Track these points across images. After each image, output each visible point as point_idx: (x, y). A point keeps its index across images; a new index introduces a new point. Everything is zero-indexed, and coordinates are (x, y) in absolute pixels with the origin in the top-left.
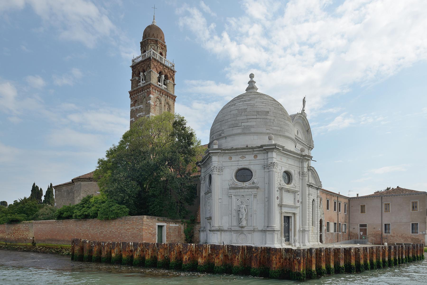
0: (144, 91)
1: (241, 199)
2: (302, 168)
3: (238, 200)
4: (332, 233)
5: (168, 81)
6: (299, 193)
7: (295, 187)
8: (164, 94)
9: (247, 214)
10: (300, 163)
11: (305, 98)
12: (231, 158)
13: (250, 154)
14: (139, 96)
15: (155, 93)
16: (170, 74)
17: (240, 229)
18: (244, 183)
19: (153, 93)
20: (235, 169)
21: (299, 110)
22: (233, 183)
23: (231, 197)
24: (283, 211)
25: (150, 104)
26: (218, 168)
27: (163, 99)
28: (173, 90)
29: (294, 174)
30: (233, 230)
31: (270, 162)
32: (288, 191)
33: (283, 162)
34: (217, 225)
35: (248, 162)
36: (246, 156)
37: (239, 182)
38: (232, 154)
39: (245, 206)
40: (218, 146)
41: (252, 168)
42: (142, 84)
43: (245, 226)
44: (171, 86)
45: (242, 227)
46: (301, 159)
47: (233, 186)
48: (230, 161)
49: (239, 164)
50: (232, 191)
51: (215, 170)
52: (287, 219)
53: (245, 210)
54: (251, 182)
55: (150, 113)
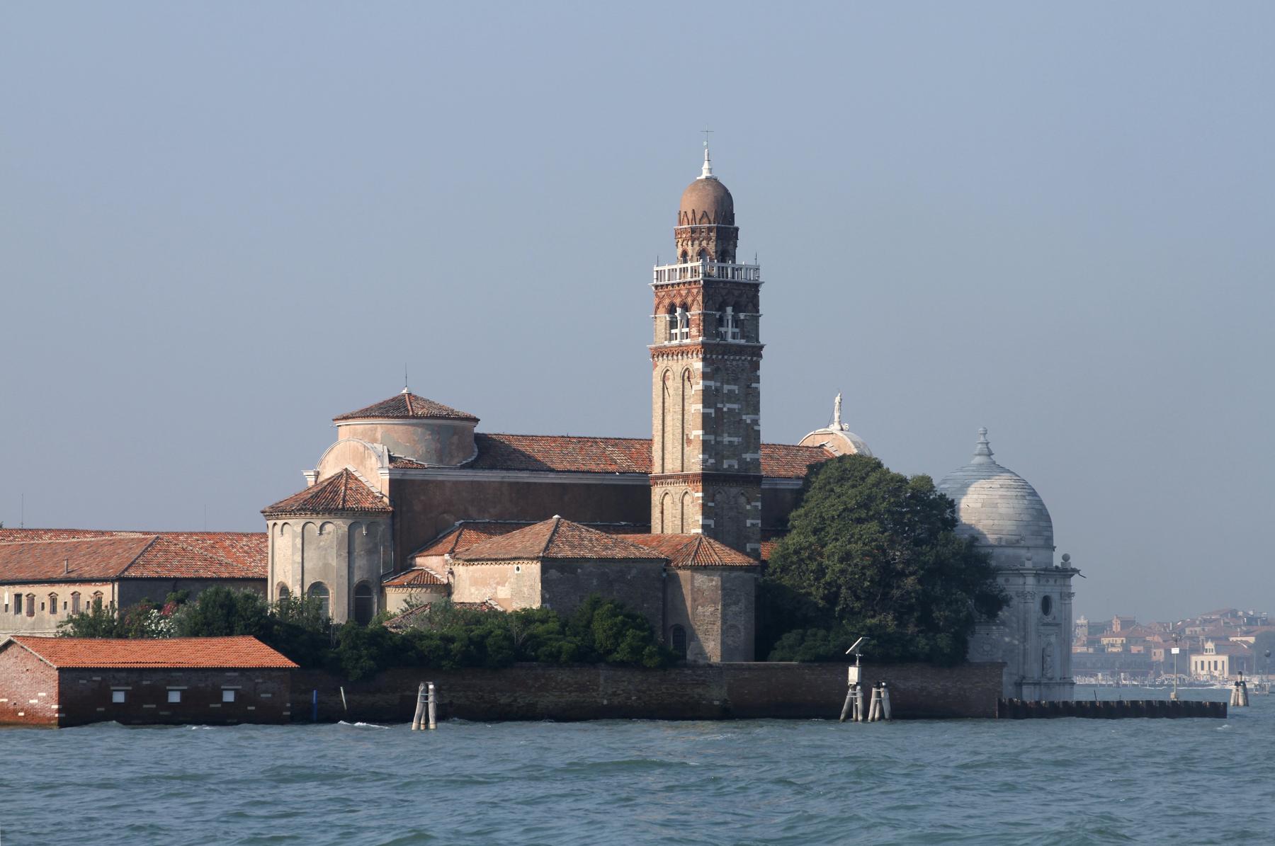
14: (728, 362)
20: (1042, 595)
45: (1051, 679)
50: (1042, 628)
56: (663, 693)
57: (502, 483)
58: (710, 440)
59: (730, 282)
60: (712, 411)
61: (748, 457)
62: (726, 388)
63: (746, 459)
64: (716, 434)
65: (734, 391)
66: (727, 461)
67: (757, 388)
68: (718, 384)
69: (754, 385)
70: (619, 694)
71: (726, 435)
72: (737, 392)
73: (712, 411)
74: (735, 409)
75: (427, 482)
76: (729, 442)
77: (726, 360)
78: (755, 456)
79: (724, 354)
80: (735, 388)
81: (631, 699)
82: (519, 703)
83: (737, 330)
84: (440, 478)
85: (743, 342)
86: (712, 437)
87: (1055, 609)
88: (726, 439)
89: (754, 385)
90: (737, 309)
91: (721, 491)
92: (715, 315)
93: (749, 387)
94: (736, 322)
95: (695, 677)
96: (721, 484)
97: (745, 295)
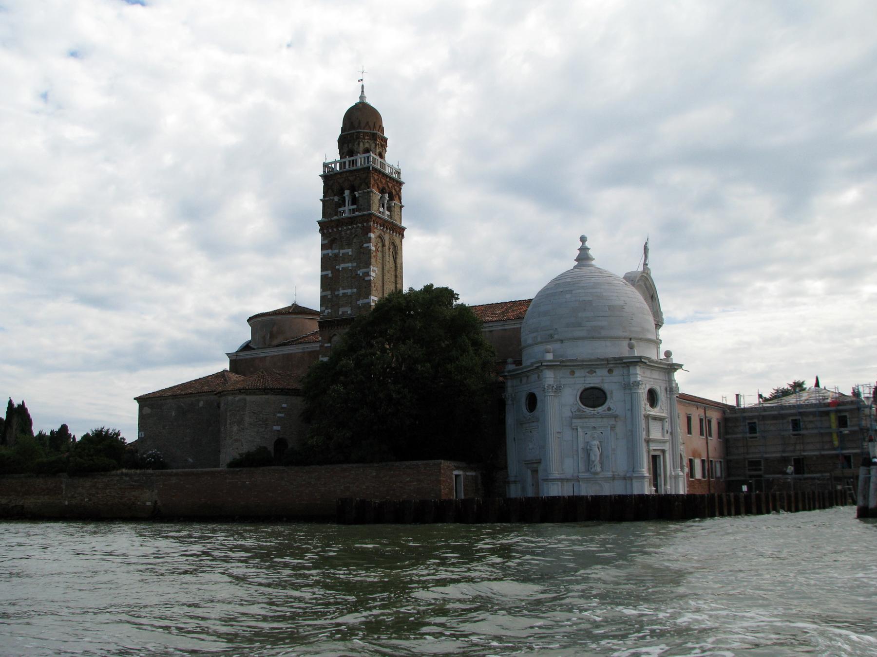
0: (356, 224)
2: (669, 381)
3: (586, 433)
4: (699, 480)
6: (667, 420)
7: (662, 411)
8: (388, 228)
9: (601, 455)
10: (666, 375)
11: (646, 243)
12: (573, 373)
13: (602, 368)
14: (343, 233)
15: (377, 228)
16: (395, 190)
17: (593, 476)
18: (596, 409)
20: (581, 388)
21: (636, 266)
22: (579, 410)
23: (577, 429)
24: (651, 448)
25: (369, 250)
26: (555, 387)
27: (387, 237)
28: (400, 216)
30: (581, 479)
31: (632, 380)
32: (655, 418)
33: (647, 377)
35: (601, 378)
36: (597, 370)
37: (587, 408)
39: (598, 442)
40: (553, 355)
41: (606, 387)
42: (347, 211)
44: (397, 209)
45: (596, 473)
46: (668, 368)
48: (571, 376)
51: (550, 390)
52: (655, 458)
53: (598, 448)
54: (605, 407)
55: (371, 266)
56: (108, 496)
57: (304, 353)
58: (327, 296)
59: (347, 172)
60: (329, 272)
61: (360, 302)
62: (342, 251)
63: (359, 305)
64: (333, 290)
65: (348, 253)
66: (342, 309)
67: (368, 247)
68: (337, 251)
69: (365, 245)
70: (76, 497)
71: (341, 289)
72: (350, 253)
73: (329, 272)
74: (348, 267)
75: (253, 359)
76: (343, 293)
77: (341, 231)
78: (366, 301)
79: (337, 226)
80: (350, 251)
81: (84, 501)
82: (12, 503)
83: (355, 207)
84: (262, 355)
85: (357, 213)
86: (329, 293)
87: (615, 401)
88: (341, 292)
89: (365, 245)
90: (353, 189)
91: (336, 333)
92: (333, 199)
93: (361, 247)
94: (354, 201)
95: (131, 483)
96: (336, 328)
97: (358, 178)
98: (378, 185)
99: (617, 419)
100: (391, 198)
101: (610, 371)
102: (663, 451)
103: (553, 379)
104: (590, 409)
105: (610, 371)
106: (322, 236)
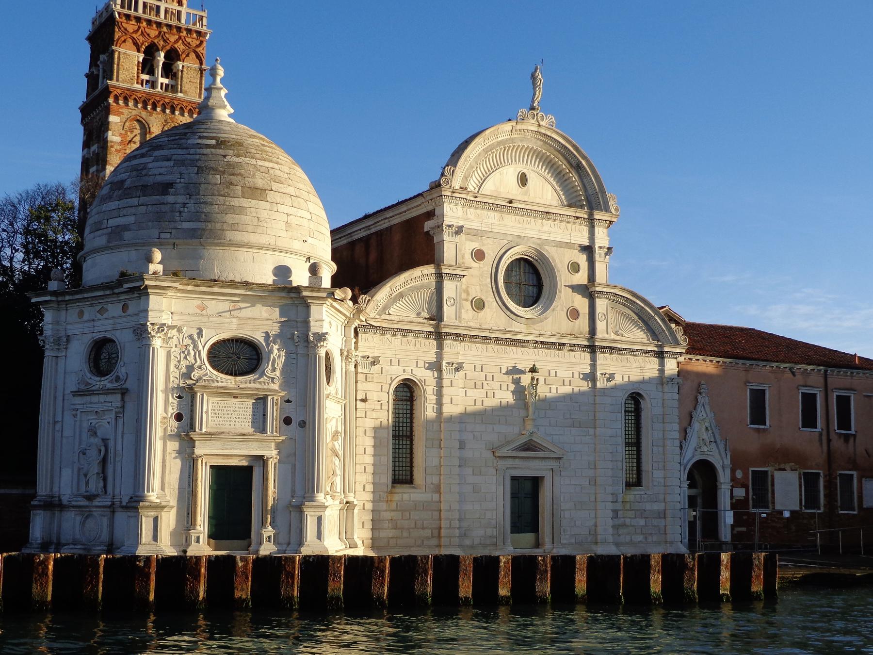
1: (97, 421)
3: (91, 423)
5: (180, 64)
12: (81, 314)
17: (86, 503)
18: (103, 379)
19: (120, 110)
29: (264, 344)
34: (44, 494)
35: (111, 321)
36: (109, 307)
38: (81, 304)
43: (95, 493)
45: (90, 498)
47: (82, 387)
48: (79, 320)
49: (97, 329)
50: (78, 400)
77: (93, 118)
98: (133, 39)
99: (127, 398)
100: (172, 56)
101: (125, 308)
102: (261, 457)
103: (50, 326)
104: (98, 379)
105: (125, 308)
106: (84, 129)
